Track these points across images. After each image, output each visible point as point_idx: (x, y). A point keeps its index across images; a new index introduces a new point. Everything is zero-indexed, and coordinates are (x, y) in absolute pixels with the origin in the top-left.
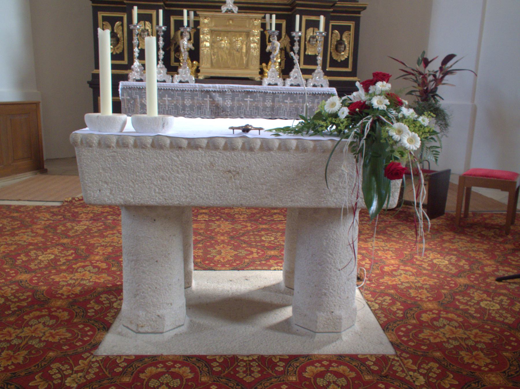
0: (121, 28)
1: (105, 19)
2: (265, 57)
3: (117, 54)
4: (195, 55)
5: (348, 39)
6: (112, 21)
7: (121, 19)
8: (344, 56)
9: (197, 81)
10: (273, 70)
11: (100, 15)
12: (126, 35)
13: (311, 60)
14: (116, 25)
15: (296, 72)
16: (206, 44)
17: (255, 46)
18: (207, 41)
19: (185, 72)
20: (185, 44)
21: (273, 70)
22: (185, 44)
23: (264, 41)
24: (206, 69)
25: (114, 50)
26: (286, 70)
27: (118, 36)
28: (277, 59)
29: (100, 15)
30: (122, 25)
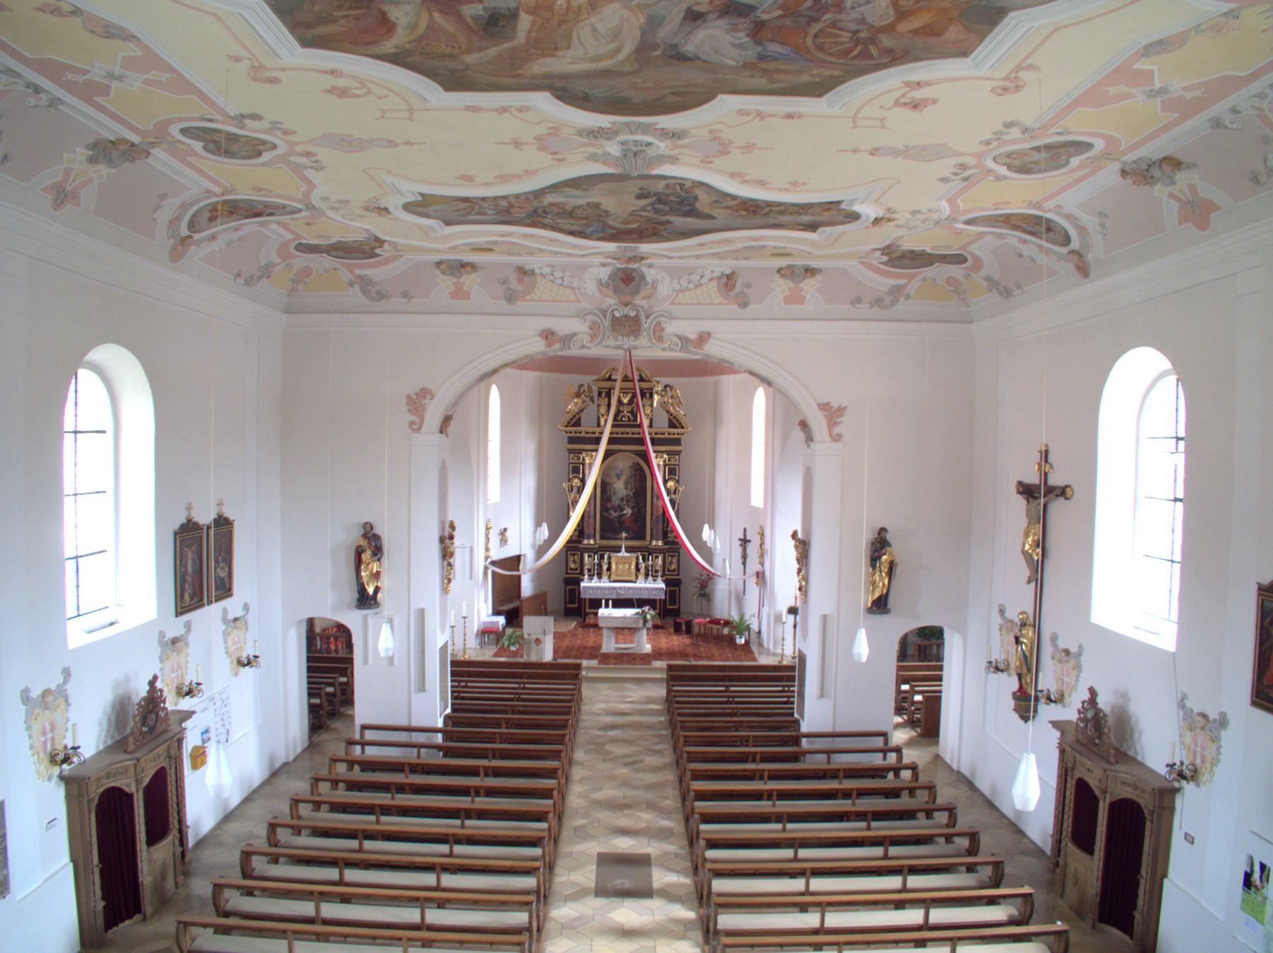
2: (638, 569)
4: (609, 569)
5: (675, 560)
8: (673, 567)
10: (641, 578)
13: (657, 571)
15: (650, 578)
16: (614, 567)
17: (633, 567)
19: (605, 578)
20: (605, 567)
21: (641, 578)
22: (605, 567)
23: (637, 564)
24: (613, 577)
26: (647, 575)
28: (642, 571)
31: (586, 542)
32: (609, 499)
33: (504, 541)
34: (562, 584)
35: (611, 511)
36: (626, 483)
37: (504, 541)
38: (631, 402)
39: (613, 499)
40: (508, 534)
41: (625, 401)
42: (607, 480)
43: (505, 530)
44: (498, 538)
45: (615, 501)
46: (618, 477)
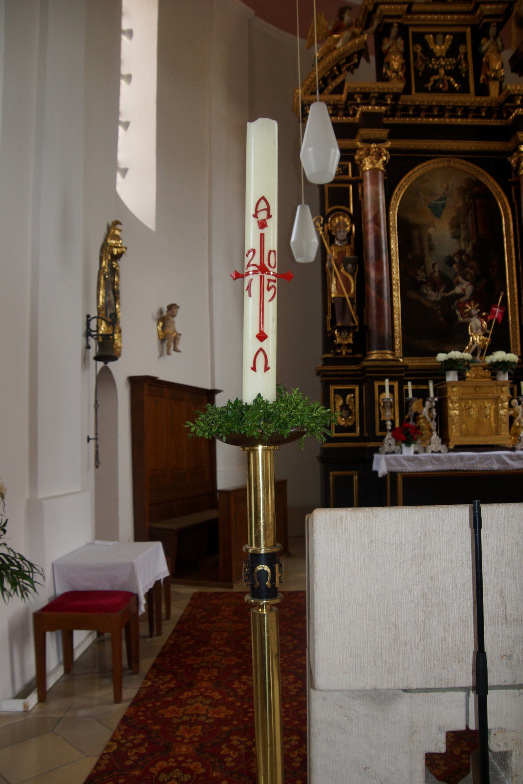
0: (353, 400)
1: (336, 392)
3: (348, 426)
6: (343, 394)
7: (353, 391)
9: (450, 451)
11: (332, 388)
12: (357, 406)
14: (348, 397)
18: (456, 410)
25: (346, 422)
27: (350, 407)
29: (332, 388)
30: (354, 397)
31: (374, 355)
32: (420, 262)
33: (168, 340)
34: (316, 468)
35: (428, 290)
36: (455, 225)
37: (168, 340)
38: (452, 52)
39: (430, 261)
40: (179, 323)
41: (439, 49)
42: (413, 218)
43: (172, 307)
44: (154, 329)
45: (434, 263)
46: (437, 211)
